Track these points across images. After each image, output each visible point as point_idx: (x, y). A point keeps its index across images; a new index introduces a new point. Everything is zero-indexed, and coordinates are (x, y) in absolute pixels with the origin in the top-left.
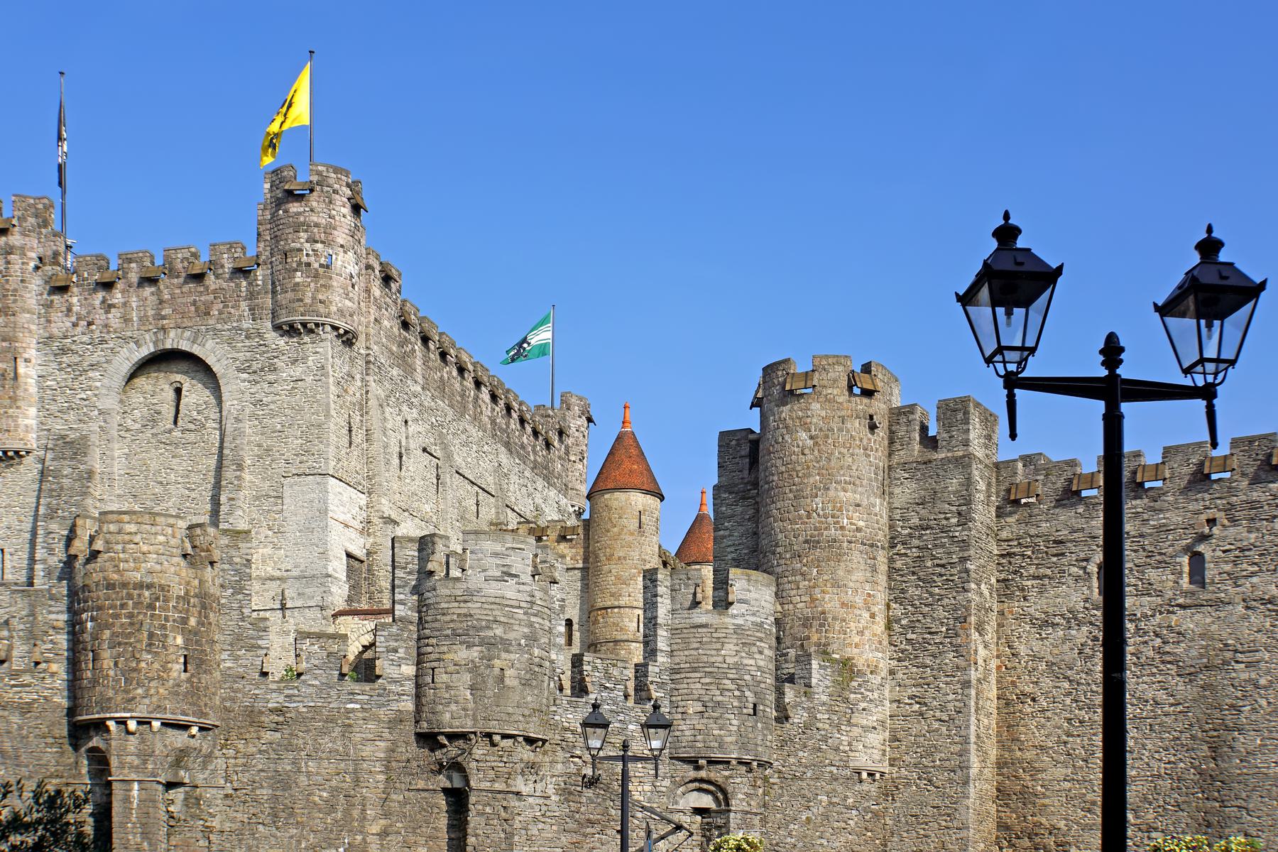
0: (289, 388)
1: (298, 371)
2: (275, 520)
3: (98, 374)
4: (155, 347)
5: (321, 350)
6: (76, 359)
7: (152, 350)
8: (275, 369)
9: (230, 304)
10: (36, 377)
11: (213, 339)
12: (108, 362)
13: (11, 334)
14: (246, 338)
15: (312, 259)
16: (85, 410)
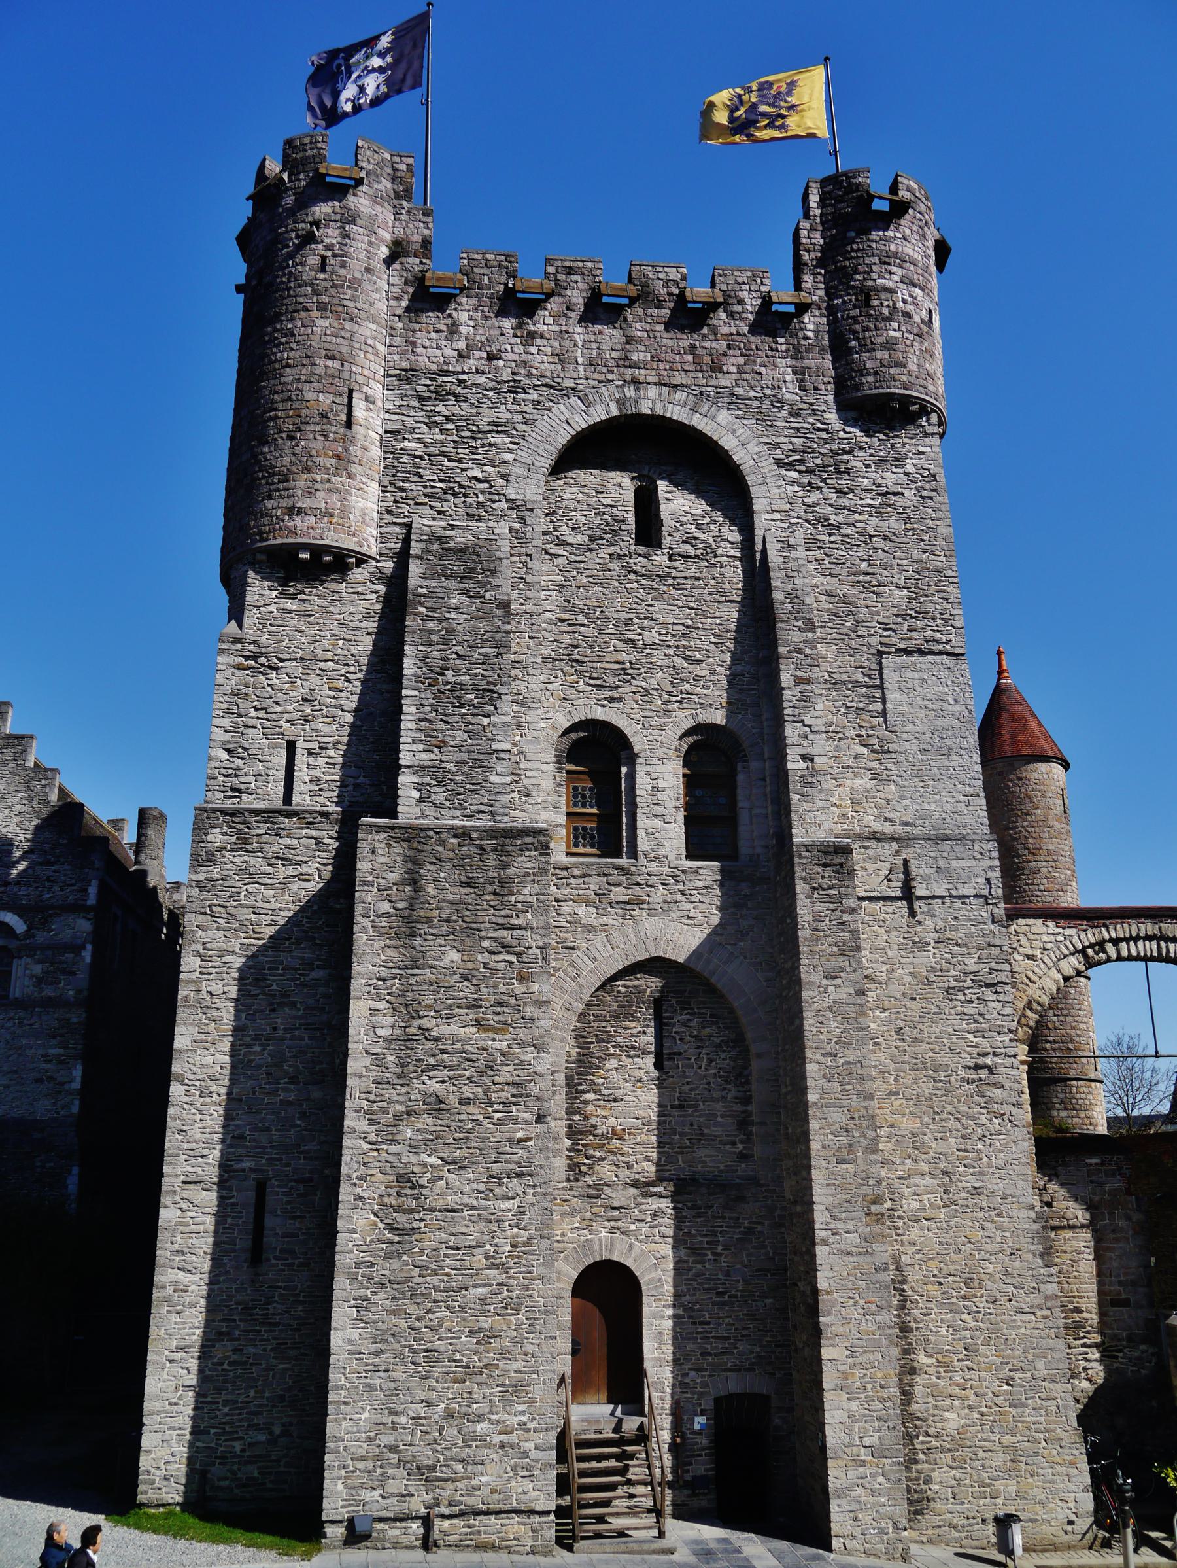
0: (876, 502)
1: (891, 478)
2: (873, 728)
3: (508, 440)
4: (620, 410)
5: (928, 450)
6: (465, 410)
7: (615, 412)
8: (848, 472)
9: (758, 360)
10: (381, 431)
11: (729, 409)
12: (526, 422)
13: (344, 349)
14: (790, 414)
15: (910, 308)
16: (481, 498)
